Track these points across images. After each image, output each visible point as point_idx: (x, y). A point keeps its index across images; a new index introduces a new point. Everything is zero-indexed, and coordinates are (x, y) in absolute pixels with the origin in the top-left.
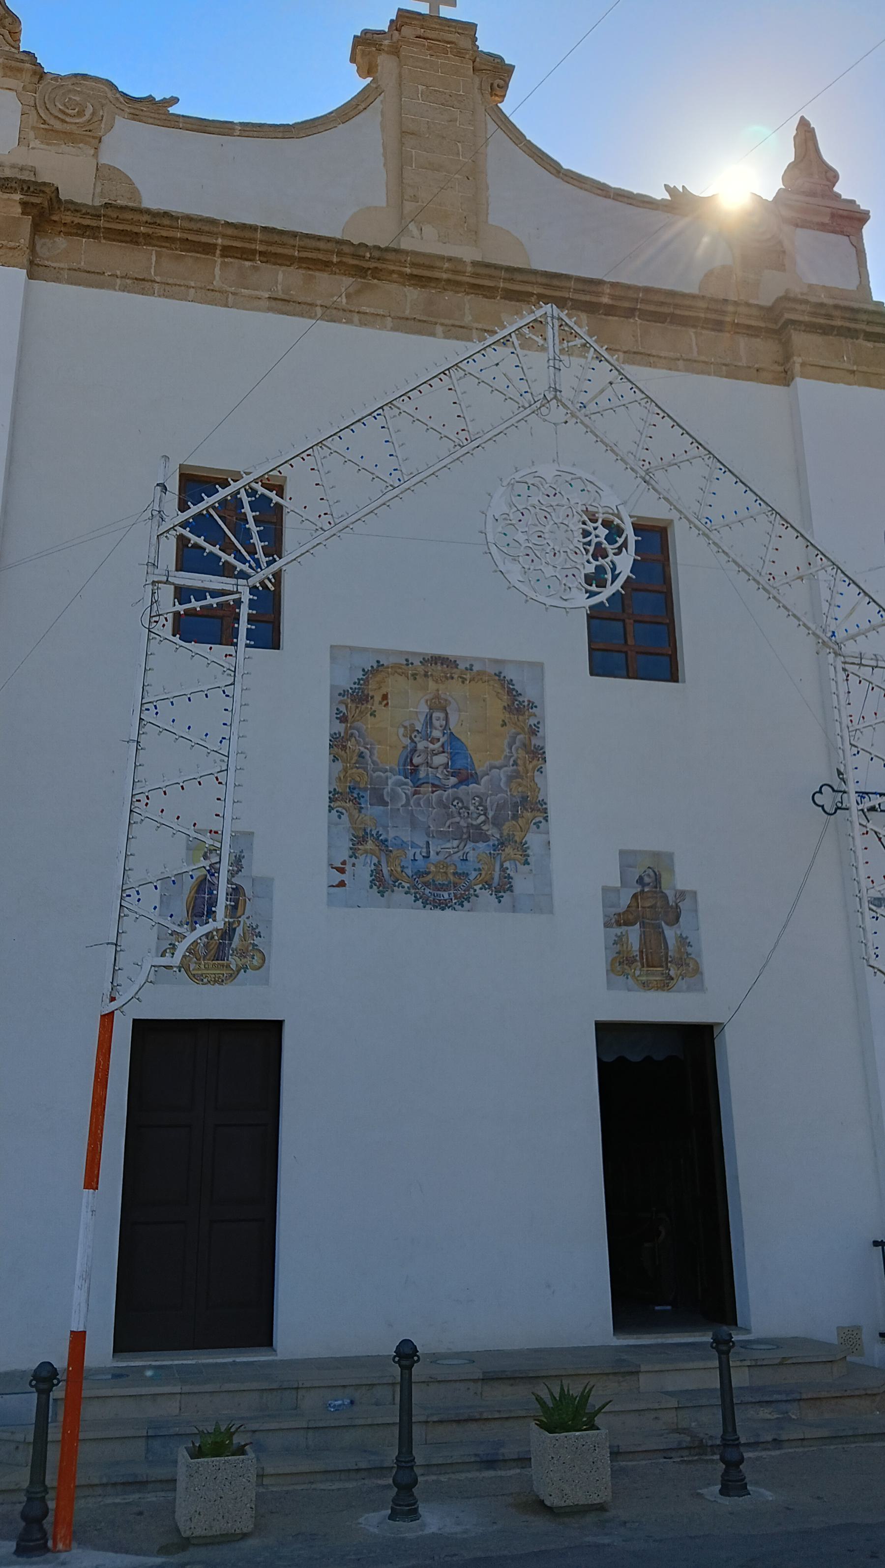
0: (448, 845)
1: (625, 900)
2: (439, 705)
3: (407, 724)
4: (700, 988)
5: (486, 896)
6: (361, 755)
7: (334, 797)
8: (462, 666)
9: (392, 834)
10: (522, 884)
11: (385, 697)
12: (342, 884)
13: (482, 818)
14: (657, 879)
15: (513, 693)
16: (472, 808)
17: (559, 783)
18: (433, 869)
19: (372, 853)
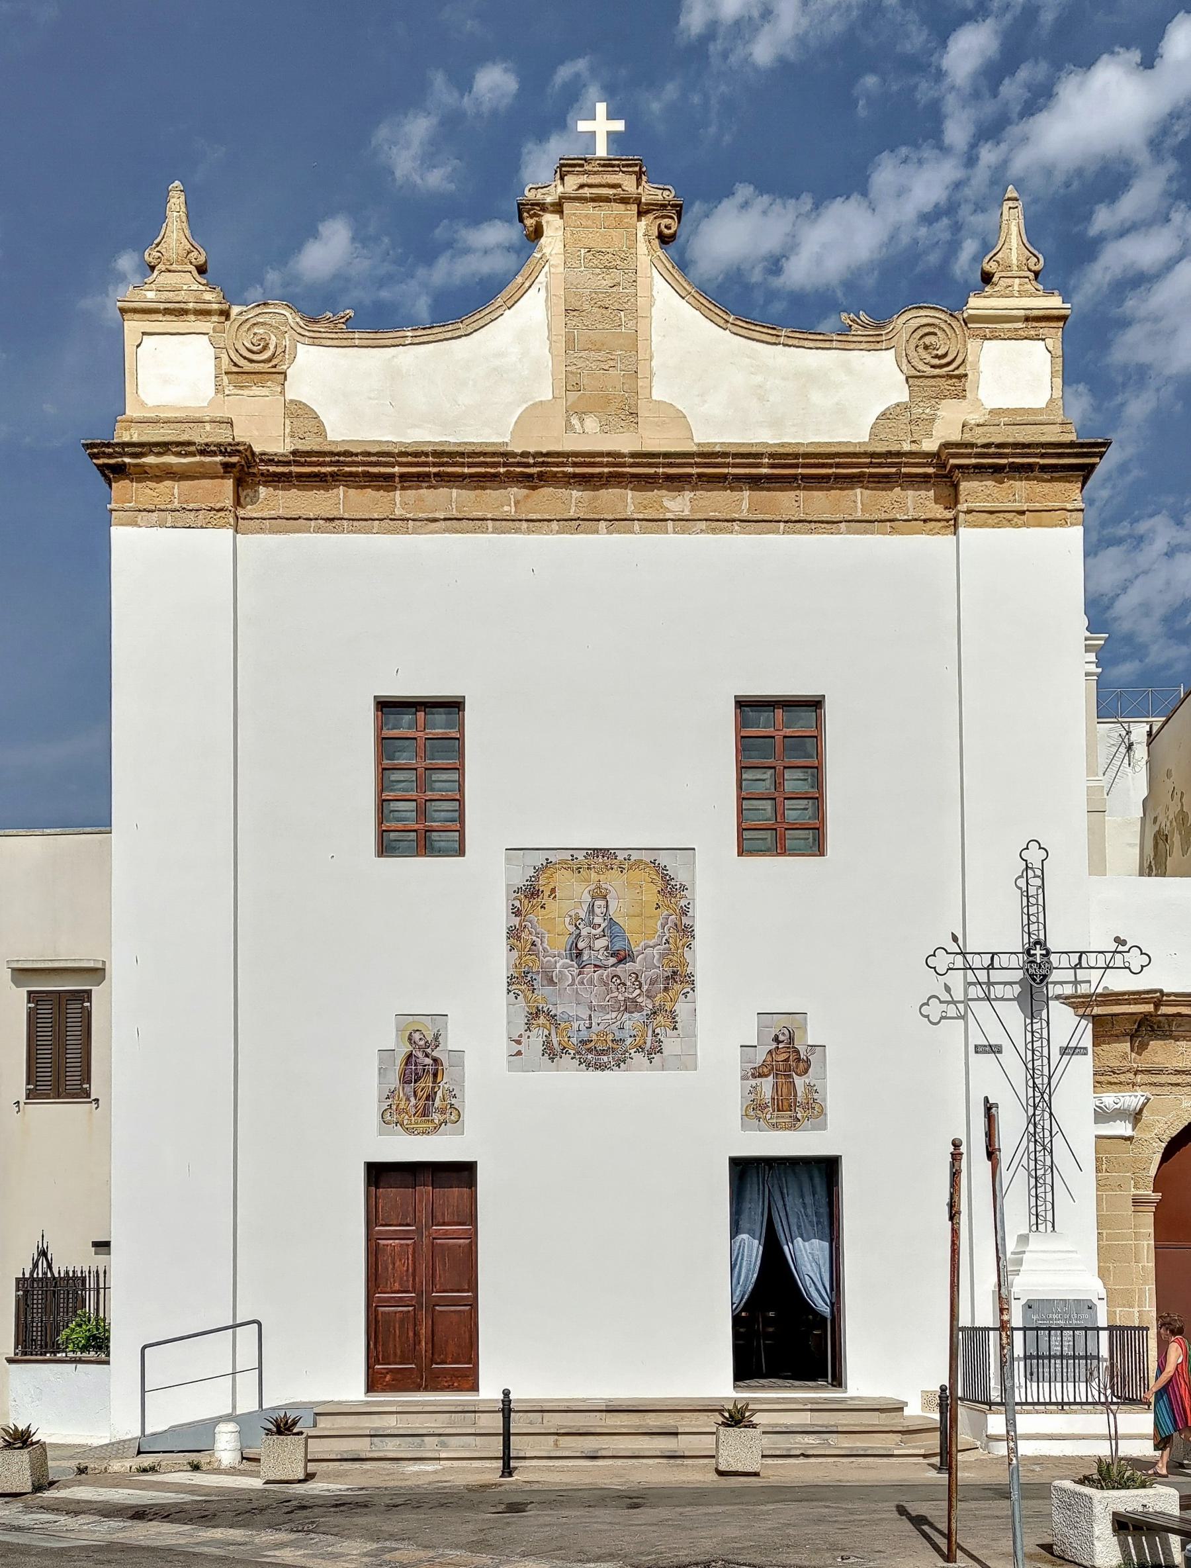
0: (608, 1017)
1: (761, 1056)
2: (600, 894)
3: (572, 913)
5: (640, 1058)
6: (533, 944)
7: (511, 981)
8: (621, 856)
9: (558, 1010)
10: (671, 1045)
11: (553, 890)
12: (519, 1053)
13: (638, 991)
14: (791, 1039)
15: (667, 879)
16: (629, 984)
17: (704, 958)
18: (594, 1037)
19: (544, 1026)
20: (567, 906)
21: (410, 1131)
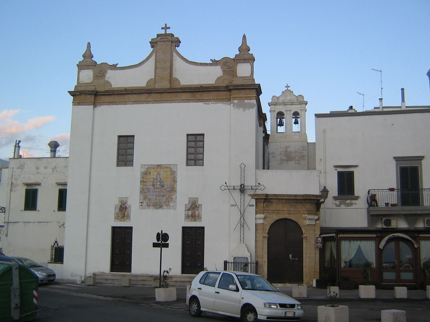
4: (201, 221)
5: (165, 207)
10: (171, 204)
11: (150, 173)
15: (171, 171)
20: (152, 176)
21: (121, 221)
